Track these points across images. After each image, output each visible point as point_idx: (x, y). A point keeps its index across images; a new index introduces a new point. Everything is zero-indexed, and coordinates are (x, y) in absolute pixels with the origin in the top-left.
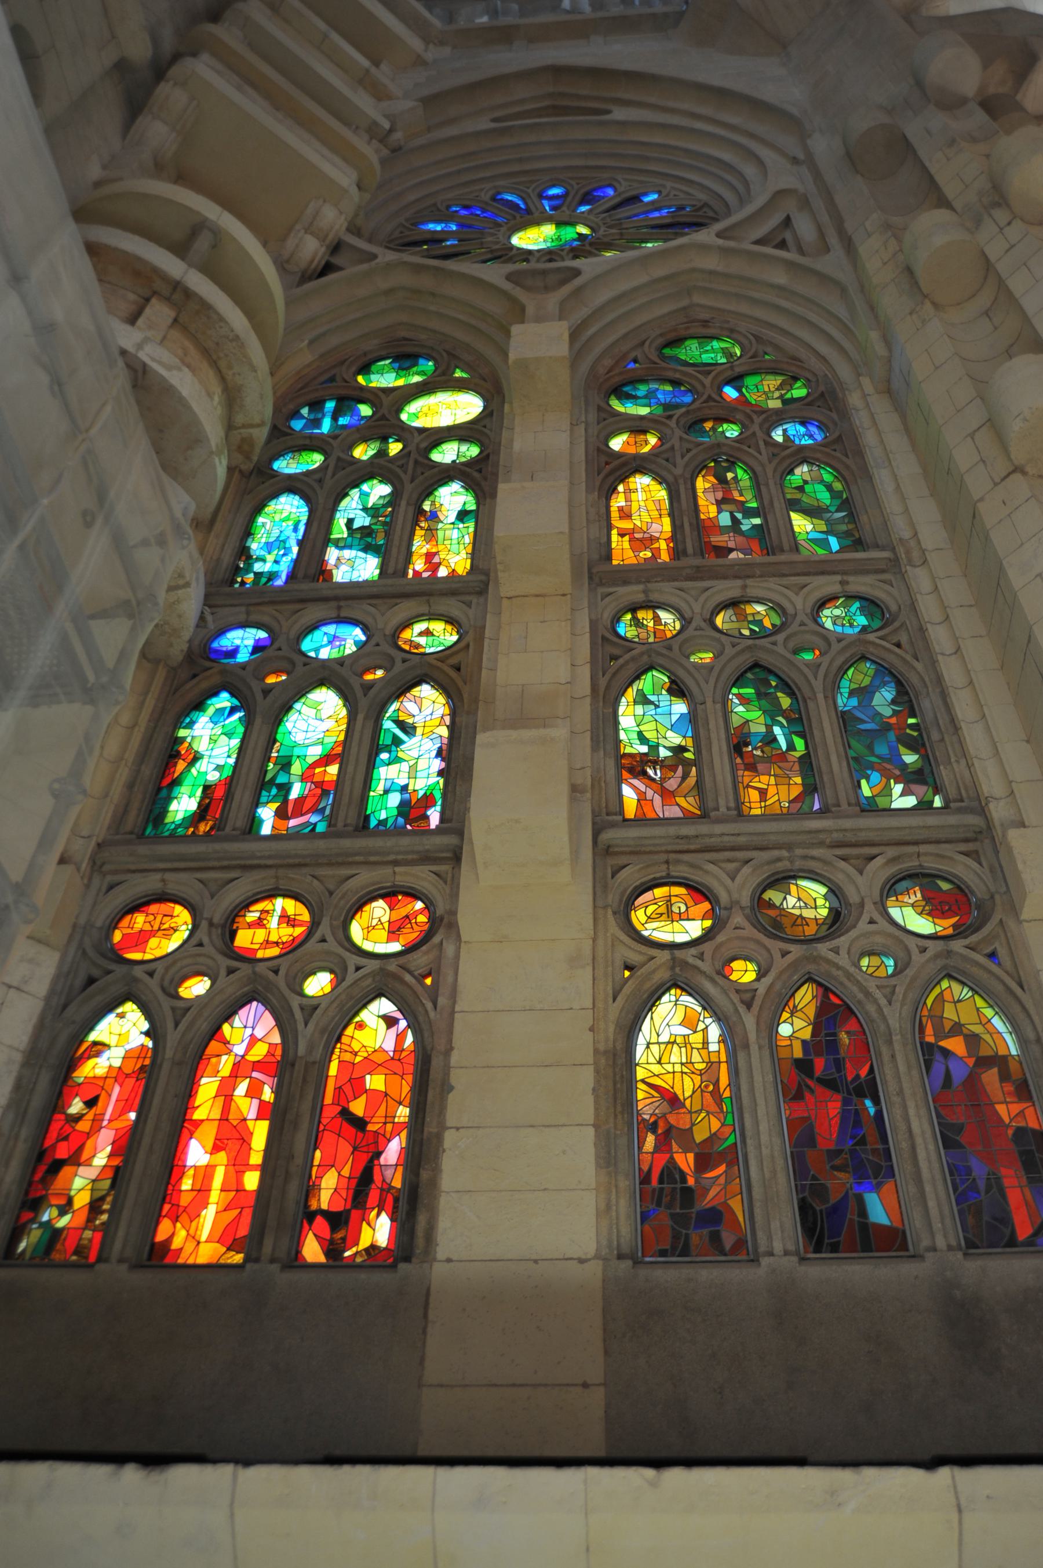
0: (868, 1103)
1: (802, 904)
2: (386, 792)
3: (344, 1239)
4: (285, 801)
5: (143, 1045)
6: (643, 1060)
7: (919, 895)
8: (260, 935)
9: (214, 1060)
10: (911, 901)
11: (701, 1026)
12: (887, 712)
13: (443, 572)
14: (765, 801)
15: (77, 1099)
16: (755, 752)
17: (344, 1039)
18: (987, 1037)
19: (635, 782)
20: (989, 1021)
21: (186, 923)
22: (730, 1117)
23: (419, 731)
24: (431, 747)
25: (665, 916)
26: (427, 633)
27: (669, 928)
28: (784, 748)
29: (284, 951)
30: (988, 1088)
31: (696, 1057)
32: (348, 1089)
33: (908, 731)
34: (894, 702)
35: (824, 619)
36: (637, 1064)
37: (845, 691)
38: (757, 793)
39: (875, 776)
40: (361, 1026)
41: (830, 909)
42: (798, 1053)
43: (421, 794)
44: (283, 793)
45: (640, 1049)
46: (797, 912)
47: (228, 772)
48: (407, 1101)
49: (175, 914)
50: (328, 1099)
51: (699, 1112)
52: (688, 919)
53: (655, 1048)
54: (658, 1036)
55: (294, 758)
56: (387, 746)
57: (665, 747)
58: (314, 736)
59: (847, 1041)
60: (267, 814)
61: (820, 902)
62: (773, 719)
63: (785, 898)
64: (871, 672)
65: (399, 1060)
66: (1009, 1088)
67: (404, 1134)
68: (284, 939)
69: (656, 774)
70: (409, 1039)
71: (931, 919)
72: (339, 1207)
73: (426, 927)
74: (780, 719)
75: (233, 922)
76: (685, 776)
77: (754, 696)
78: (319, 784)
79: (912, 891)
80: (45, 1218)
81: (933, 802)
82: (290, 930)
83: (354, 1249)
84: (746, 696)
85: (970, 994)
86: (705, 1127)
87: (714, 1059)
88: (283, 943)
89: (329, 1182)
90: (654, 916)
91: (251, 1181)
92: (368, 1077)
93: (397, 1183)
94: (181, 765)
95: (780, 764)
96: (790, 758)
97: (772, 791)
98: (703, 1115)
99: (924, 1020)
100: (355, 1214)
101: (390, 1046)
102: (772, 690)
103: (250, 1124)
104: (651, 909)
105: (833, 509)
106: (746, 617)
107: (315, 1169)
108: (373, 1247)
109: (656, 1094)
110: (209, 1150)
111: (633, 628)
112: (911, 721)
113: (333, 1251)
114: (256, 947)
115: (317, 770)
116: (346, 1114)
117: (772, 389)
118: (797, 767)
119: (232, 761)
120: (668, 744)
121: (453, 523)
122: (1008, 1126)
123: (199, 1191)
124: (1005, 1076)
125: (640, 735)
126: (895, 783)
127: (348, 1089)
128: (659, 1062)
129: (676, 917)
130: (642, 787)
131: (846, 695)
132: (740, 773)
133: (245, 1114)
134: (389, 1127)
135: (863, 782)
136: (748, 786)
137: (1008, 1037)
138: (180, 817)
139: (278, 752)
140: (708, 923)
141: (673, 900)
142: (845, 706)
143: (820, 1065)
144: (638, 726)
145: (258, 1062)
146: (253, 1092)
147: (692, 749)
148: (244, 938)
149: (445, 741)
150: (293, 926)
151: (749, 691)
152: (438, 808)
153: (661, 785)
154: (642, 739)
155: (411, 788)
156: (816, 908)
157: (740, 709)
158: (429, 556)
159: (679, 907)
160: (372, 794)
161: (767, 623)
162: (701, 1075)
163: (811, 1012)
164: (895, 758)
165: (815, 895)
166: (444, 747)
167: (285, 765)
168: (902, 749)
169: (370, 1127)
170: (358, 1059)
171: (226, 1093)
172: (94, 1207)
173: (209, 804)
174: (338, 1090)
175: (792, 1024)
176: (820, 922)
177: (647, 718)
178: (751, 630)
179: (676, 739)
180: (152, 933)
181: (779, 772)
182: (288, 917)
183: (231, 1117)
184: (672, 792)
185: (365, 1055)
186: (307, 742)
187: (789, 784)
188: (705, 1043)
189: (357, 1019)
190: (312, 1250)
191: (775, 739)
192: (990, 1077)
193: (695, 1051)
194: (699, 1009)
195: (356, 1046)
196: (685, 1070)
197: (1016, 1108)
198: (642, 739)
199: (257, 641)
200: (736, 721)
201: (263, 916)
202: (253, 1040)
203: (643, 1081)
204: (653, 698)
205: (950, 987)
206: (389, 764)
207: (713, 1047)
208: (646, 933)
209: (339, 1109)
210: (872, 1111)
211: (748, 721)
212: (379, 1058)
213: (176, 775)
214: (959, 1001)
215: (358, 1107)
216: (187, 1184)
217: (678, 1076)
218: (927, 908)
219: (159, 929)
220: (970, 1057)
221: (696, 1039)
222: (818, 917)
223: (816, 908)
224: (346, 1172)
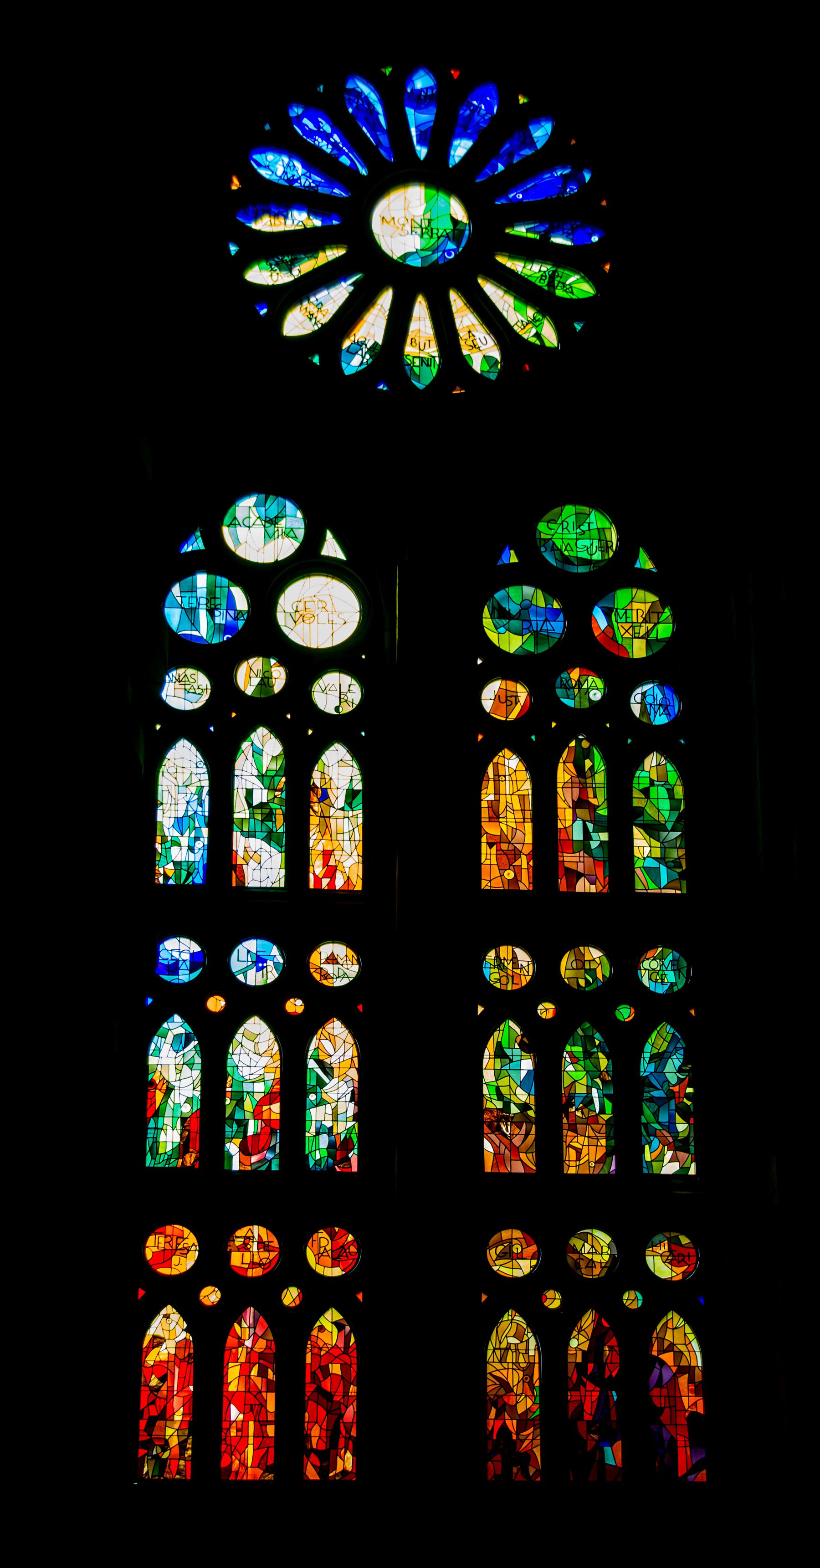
0: (614, 1393)
1: (594, 1251)
2: (318, 1133)
4: (245, 1136)
5: (185, 1338)
6: (491, 1360)
7: (666, 1247)
10: (661, 1252)
11: (525, 1338)
12: (673, 1078)
13: (339, 883)
14: (580, 1160)
15: (153, 1376)
16: (577, 1112)
17: (313, 1339)
18: (686, 1354)
19: (493, 1136)
20: (690, 1342)
21: (194, 1244)
22: (538, 1398)
24: (345, 1089)
25: (508, 1255)
26: (332, 959)
27: (510, 1265)
28: (597, 1111)
29: (266, 1271)
30: (681, 1388)
31: (521, 1359)
33: (685, 1100)
34: (680, 1070)
35: (643, 972)
36: (488, 1362)
37: (647, 1056)
38: (574, 1151)
39: (656, 1142)
40: (322, 1328)
41: (610, 1255)
42: (579, 1359)
43: (343, 1136)
44: (242, 1129)
45: (490, 1352)
46: (589, 1256)
47: (197, 1106)
48: (355, 1383)
49: (185, 1236)
50: (308, 1379)
51: (520, 1395)
52: (522, 1258)
53: (498, 1352)
54: (500, 1343)
55: (245, 1094)
56: (314, 1086)
57: (515, 1104)
58: (257, 1072)
59: (608, 1352)
60: (233, 1147)
61: (605, 1249)
62: (592, 1079)
63: (584, 1245)
64: (669, 1037)
66: (692, 1387)
67: (355, 1403)
68: (264, 1261)
69: (507, 1130)
70: (353, 1340)
71: (670, 1266)
72: (323, 1447)
73: (356, 1257)
74: (598, 1080)
75: (227, 1246)
76: (527, 1134)
77: (581, 1055)
78: (268, 1122)
79: (662, 1244)
81: (689, 1168)
82: (266, 1255)
83: (334, 1472)
84: (577, 1055)
85: (683, 1323)
86: (524, 1404)
87: (532, 1361)
88: (264, 1265)
89: (315, 1432)
90: (501, 1255)
91: (271, 1430)
92: (330, 1365)
93: (354, 1433)
94: (159, 1096)
95: (592, 1125)
96: (601, 1121)
97: (585, 1151)
98: (523, 1397)
99: (654, 1339)
100: (333, 1452)
101: (341, 1345)
102: (595, 1050)
103: (264, 1394)
104: (500, 1248)
105: (669, 826)
106: (584, 965)
107: (306, 1424)
108: (344, 1472)
109: (498, 1383)
111: (496, 970)
112: (690, 1090)
113: (323, 1471)
114: (246, 1266)
115: (265, 1108)
116: (320, 1390)
117: (641, 620)
118: (604, 1130)
119: (197, 1094)
120: (518, 1102)
121: (342, 809)
122: (686, 1411)
124: (691, 1380)
125: (498, 1088)
126: (668, 1150)
128: (500, 1362)
129: (514, 1255)
130: (497, 1142)
131: (647, 1060)
132: (565, 1132)
133: (260, 1388)
135: (647, 1147)
136: (569, 1146)
137: (699, 1355)
138: (169, 1148)
139: (231, 1087)
140: (534, 1262)
141: (514, 1241)
142: (645, 1072)
143: (591, 1367)
144: (497, 1080)
146: (262, 1373)
147: (533, 1107)
148: (236, 1259)
149: (356, 1085)
150: (269, 1251)
151: (578, 1049)
152: (356, 1151)
153: (511, 1140)
154: (500, 1096)
155: (335, 1131)
156: (602, 1254)
157: (570, 1068)
158: (327, 855)
159: (517, 1249)
160: (307, 1134)
161: (600, 976)
162: (523, 1371)
163: (590, 1331)
164: (671, 1126)
165: (602, 1244)
166: (356, 1091)
167: (240, 1103)
168: (678, 1119)
169: (337, 1399)
170: (323, 1353)
171: (245, 1374)
173: (189, 1135)
174: (313, 1374)
175: (578, 1340)
176: (603, 1265)
177: (504, 1073)
178: (587, 981)
179: (522, 1096)
180: (173, 1252)
181: (591, 1133)
182: (264, 1243)
183: (251, 1390)
184: (518, 1148)
186: (252, 1077)
187: (597, 1146)
188: (527, 1350)
189: (318, 1324)
190: (311, 1473)
191: (591, 1102)
192: (683, 1380)
193: (521, 1355)
194: (525, 1326)
195: (321, 1344)
196: (515, 1367)
197: (693, 1399)
198: (500, 1096)
199: (193, 955)
200: (566, 1082)
201: (247, 1241)
202: (256, 1338)
203: (490, 1373)
204: (508, 1052)
205: (672, 1318)
206: (317, 1106)
207: (532, 1353)
208: (495, 1268)
209: (315, 1386)
210: (615, 1398)
211: (575, 1081)
212: (336, 1353)
213: (157, 1107)
214: (676, 1328)
215: (327, 1385)
217: (510, 1371)
218: (670, 1258)
220: (674, 1366)
221: (522, 1347)
222: (603, 1261)
223: (602, 1254)
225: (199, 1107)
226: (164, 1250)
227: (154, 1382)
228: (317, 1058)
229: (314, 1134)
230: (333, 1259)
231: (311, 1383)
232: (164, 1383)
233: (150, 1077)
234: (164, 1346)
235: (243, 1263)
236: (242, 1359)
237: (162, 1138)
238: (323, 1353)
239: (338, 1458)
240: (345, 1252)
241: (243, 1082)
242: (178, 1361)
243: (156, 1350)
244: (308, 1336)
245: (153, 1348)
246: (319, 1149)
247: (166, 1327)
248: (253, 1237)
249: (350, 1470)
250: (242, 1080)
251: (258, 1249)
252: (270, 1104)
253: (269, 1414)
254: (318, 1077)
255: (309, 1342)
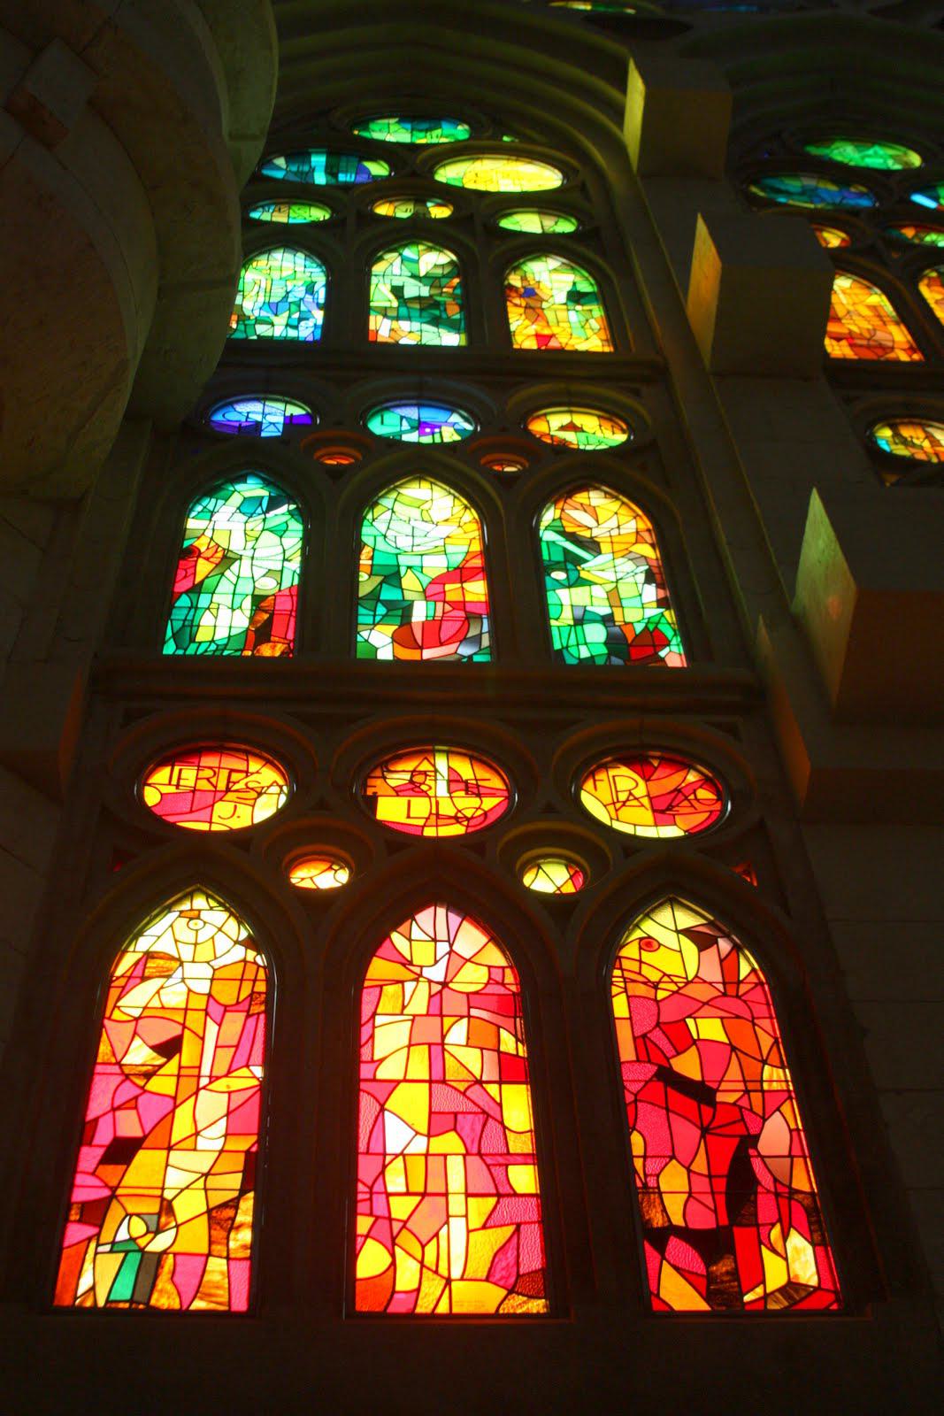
3: (734, 1274)
5: (244, 961)
8: (421, 807)
9: (390, 990)
23: (605, 548)
32: (658, 1037)
50: (627, 1051)
65: (738, 997)
68: (469, 813)
72: (704, 1221)
80: (123, 1235)
88: (468, 819)
89: (673, 1180)
91: (524, 1179)
92: (690, 1022)
94: (203, 568)
108: (792, 1287)
110: (424, 1130)
114: (421, 822)
123: (424, 1195)
127: (658, 1037)
134: (756, 1098)
145: (476, 993)
150: (479, 795)
167: (393, 577)
172: (219, 1218)
174: (641, 1041)
185: (674, 988)
195: (654, 976)
209: (651, 1070)
215: (688, 1065)
216: (394, 1180)
219: (228, 790)
224: (700, 1165)
225: (296, 582)
226: (194, 791)
227: (140, 1054)
228: (562, 529)
229: (572, 623)
230: (654, 811)
231: (638, 1060)
232: (169, 1058)
233: (186, 544)
234: (178, 974)
235: (409, 817)
236: (419, 1005)
237: (207, 620)
238: (661, 995)
239: (765, 1252)
240: (686, 798)
241: (397, 555)
242: (216, 1011)
243: (150, 987)
244: (612, 959)
245: (143, 979)
246: (586, 644)
247: (189, 937)
248: (436, 771)
249: (814, 1281)
250: (398, 551)
251: (450, 792)
252: (462, 582)
253: (510, 1136)
254: (566, 551)
255: (617, 972)
